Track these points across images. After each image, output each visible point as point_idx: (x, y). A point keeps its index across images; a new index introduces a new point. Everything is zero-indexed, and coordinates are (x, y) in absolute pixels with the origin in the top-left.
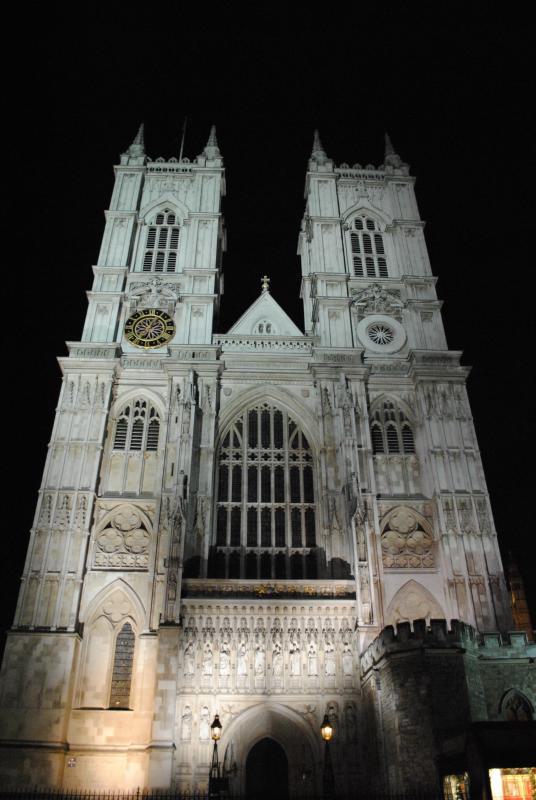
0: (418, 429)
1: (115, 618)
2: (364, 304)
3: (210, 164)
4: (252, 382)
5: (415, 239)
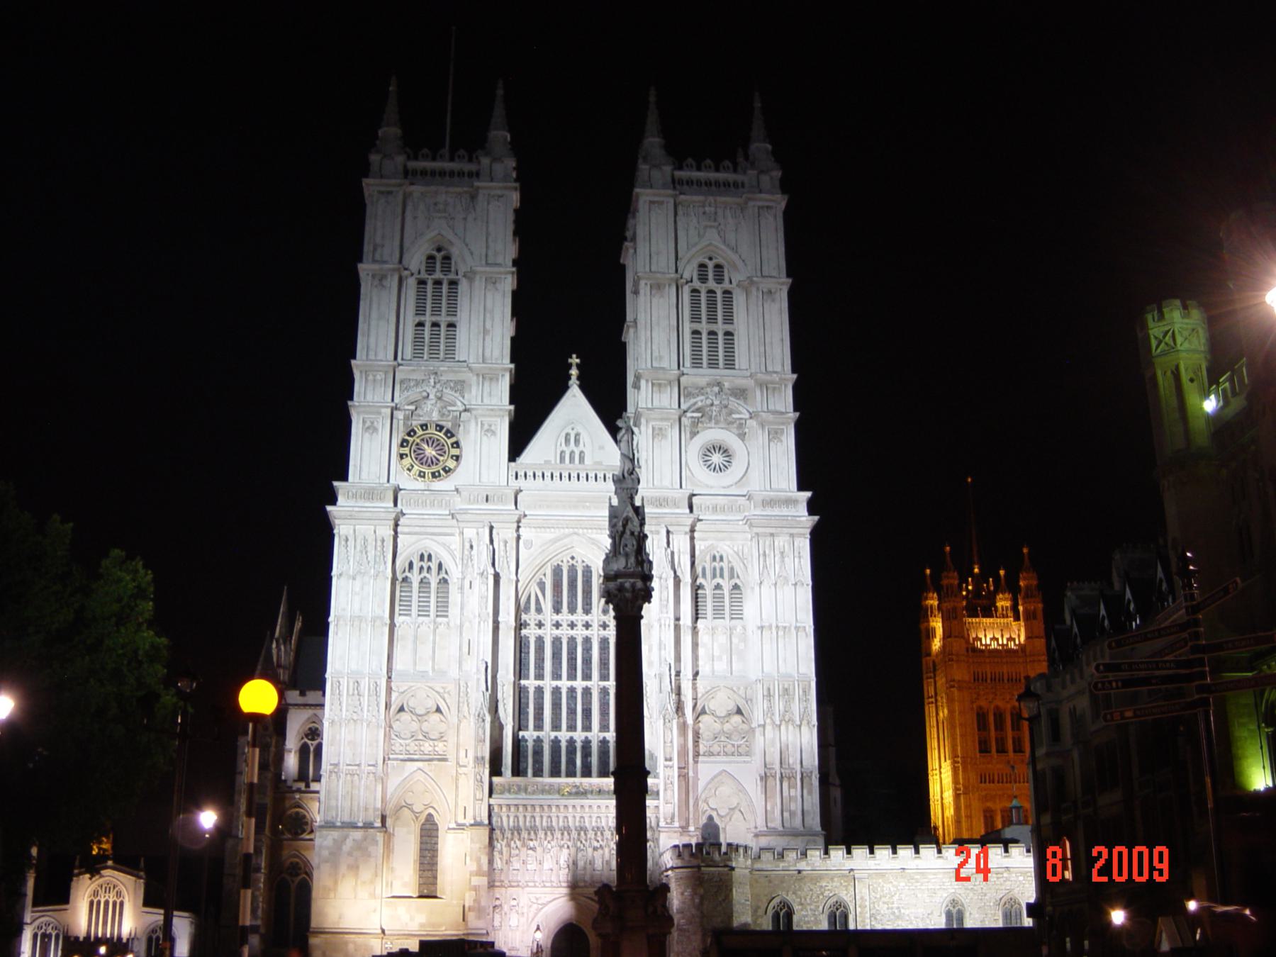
0: (749, 591)
1: (417, 808)
2: (700, 415)
3: (498, 168)
4: (557, 530)
5: (776, 306)
